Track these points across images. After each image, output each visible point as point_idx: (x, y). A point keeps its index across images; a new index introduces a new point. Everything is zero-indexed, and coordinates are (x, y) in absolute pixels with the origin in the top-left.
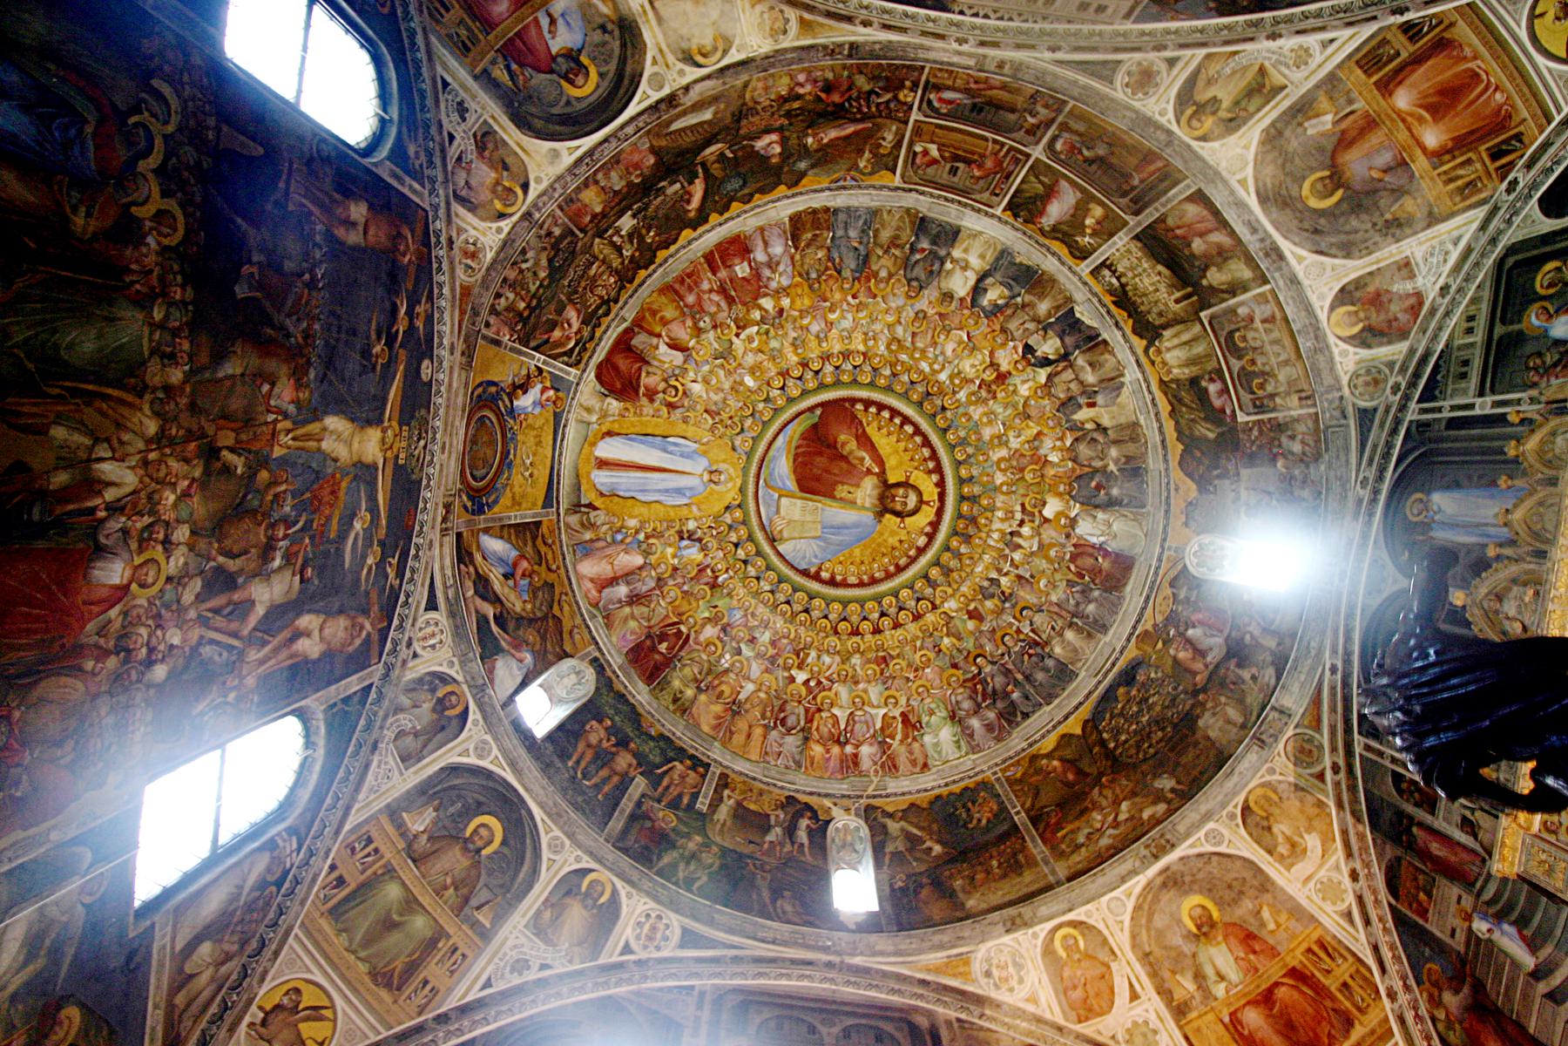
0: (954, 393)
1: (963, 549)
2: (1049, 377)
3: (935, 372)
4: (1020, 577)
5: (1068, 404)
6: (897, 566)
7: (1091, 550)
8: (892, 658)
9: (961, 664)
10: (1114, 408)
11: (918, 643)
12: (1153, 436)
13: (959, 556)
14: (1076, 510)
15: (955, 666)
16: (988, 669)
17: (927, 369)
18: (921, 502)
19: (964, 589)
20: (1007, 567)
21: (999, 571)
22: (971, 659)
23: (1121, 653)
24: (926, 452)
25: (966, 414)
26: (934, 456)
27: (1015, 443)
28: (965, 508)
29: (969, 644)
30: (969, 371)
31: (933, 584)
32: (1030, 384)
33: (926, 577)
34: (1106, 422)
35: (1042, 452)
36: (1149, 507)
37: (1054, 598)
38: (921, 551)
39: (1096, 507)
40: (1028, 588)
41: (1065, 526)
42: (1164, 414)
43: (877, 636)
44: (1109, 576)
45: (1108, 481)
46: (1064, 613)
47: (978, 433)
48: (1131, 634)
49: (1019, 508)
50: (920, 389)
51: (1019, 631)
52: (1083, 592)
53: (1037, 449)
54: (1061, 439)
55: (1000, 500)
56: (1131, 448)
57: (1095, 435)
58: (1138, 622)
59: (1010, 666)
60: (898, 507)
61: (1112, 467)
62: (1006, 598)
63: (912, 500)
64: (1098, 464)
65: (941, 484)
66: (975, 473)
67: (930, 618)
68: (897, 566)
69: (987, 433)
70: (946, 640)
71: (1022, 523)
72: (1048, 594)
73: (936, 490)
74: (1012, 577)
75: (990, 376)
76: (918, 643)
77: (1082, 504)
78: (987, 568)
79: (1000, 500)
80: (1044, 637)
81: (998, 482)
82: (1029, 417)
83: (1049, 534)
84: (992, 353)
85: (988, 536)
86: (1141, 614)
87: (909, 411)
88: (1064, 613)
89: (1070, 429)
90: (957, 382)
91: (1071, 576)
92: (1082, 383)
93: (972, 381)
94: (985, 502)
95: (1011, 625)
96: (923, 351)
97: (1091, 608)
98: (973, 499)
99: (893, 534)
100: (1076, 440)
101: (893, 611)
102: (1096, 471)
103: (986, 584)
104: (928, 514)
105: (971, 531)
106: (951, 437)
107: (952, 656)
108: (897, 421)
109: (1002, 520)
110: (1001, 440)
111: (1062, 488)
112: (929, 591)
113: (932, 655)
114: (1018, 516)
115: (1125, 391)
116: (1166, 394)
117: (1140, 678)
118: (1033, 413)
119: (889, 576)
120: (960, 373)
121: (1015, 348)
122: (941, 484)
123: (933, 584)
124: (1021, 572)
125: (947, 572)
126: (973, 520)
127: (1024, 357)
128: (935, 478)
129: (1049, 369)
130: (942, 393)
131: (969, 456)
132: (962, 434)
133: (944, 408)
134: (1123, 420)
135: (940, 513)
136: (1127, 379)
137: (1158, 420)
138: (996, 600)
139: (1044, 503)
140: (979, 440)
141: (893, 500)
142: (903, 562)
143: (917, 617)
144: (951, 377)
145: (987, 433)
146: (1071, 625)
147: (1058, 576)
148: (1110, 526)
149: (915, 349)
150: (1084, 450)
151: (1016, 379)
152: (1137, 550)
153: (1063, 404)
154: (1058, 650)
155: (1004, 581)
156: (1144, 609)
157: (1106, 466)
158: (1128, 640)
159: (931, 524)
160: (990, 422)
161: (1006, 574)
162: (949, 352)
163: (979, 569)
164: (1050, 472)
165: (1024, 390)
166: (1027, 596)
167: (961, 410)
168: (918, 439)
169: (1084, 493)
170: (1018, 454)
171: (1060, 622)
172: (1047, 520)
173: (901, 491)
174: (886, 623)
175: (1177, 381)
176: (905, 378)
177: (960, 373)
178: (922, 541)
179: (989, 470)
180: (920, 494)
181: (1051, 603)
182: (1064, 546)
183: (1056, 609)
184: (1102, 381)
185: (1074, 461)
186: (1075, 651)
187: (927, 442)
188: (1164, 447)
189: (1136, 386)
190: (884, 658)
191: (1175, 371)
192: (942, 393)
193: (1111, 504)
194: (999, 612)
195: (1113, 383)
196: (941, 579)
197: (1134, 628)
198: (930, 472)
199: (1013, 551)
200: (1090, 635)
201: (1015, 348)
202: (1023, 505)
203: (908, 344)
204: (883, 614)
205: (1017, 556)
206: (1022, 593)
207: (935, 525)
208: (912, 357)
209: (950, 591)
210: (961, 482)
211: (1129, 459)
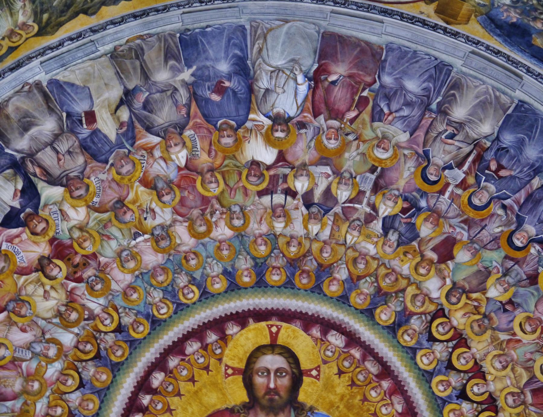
0: (92, 317)
1: (342, 274)
2: (53, 181)
3: (61, 352)
4: (376, 188)
5: (94, 149)
6: (381, 376)
7: (320, 92)
8: (532, 379)
9: (528, 269)
10: (92, 86)
11: (503, 337)
12: (131, 29)
13: (353, 281)
14: (258, 118)
15: (533, 279)
16: (531, 229)
17: (58, 366)
18: (273, 347)
19: (406, 269)
20: (363, 208)
21: (369, 219)
22: (519, 255)
23: (477, 43)
24: (193, 347)
25: (125, 294)
26: (197, 334)
27: (164, 216)
28: (275, 278)
29: (494, 257)
30: (57, 298)
31: (403, 318)
32: (67, 208)
33: (392, 330)
34: (116, 93)
35: (173, 174)
36: (243, 21)
37: (403, 137)
38: (353, 339)
39: (251, 90)
40: (393, 175)
41: (288, 131)
42: (93, 21)
43: (501, 403)
44: (358, 63)
45: (209, 79)
46: (426, 122)
47: (153, 273)
48: (445, 30)
49: (266, 200)
50: (90, 371)
51: (463, 185)
52: (388, 98)
53: (169, 183)
54: (150, 150)
55: (257, 228)
56: (152, 56)
57: (138, 103)
58: (424, 23)
59: (522, 196)
60: (285, 382)
61: (187, 75)
62: (411, 207)
63: (272, 361)
64: (183, 95)
65: (242, 319)
66: (217, 269)
67: (459, 319)
68: (381, 376)
69: (151, 258)
70: (493, 292)
71: (291, 193)
72: (398, 146)
73: (252, 325)
74: (378, 199)
75: (60, 269)
76: (503, 337)
77: (249, 110)
78: (368, 237)
79: (257, 228)
80: (467, 149)
81: (228, 233)
82: (121, 202)
83: (302, 150)
84: (23, 272)
85: (316, 238)
86: (412, 20)
87: (128, 383)
88: (426, 122)
89: (133, 139)
90: (74, 316)
91: (366, 116)
92: (56, 137)
93: (71, 294)
94: (263, 250)
95: (453, 198)
96: (29, 377)
97: (413, 86)
98: (260, 268)
99: (329, 387)
100: (149, 129)
101: (455, 380)
102: (194, 96)
103: (393, 237)
104: (293, 336)
105: (311, 265)
106: (164, 311)
107: (518, 283)
108: (146, 400)
109: (288, 220)
110: (161, 237)
111: (227, 141)
112: (416, 324)
113: (520, 316)
114: (279, 198)
115: (63, 76)
116: (61, 24)
117: (514, 17)
118: (112, 196)
119: (399, 388)
120: (59, 314)
121: (10, 240)
122: (242, 319)
123: (403, 318)
124: (367, 187)
125: (381, 297)
126: (293, 264)
127: (24, 224)
128: (232, 329)
129: (41, 186)
130: (94, 336)
131: (192, 281)
132: (157, 295)
133: (120, 329)
134: (110, 73)
135: (287, 316)
136: (43, 78)
137: (103, 28)
138: (419, 221)
139: (255, 163)
140: (164, 269)
141: (275, 391)
142: (373, 368)
143: (460, 340)
144: (67, 325)
145: (151, 258)
146: (442, 112)
147: (368, 134)
148: (279, 70)
149: (25, 391)
150: (165, 115)
151: (63, 230)
152: (312, 30)
153: (94, 157)
154: (486, 128)
155: (386, 209)
156: (402, 17)
157: (185, 84)
158: (455, 35)
159: (306, 329)
160: (133, 257)
161: (374, 208)
162: (28, 337)
163: (371, 249)
164: (204, 159)
165: (78, 214)
166: (405, 175)
167: (119, 302)
168: (173, 362)
169: (231, 107)
170: (181, 211)
171: (441, 127)
172: (281, 158)
173: (259, 380)
174: (475, 389)
175: (37, 15)
176: (75, 398)
177: (59, 314)
178: (336, 340)
179: (211, 248)
180: (260, 351)
181: (412, 140)
182: (318, 131)
183: (420, 134)
184: (51, 110)
185: (181, 128)
186: (483, 105)
187: (177, 348)
188: (145, 13)
189: (53, 64)
190: (534, 392)
191: (21, 19)
192: (94, 336)
193: (243, 69)
194: (436, 216)
195: (52, 95)
196: (394, 306)
197: (435, 27)
198: (224, 338)
199: (336, 201)
200: (457, 86)
201: (10, 240)
202: (261, 194)
203: (18, 404)
204: (463, 395)
205: (343, 194)
206: (401, 184)
207: (307, 321)
208: (39, 394)
209: (411, 291)
210: (234, 287)
211: (169, 55)
